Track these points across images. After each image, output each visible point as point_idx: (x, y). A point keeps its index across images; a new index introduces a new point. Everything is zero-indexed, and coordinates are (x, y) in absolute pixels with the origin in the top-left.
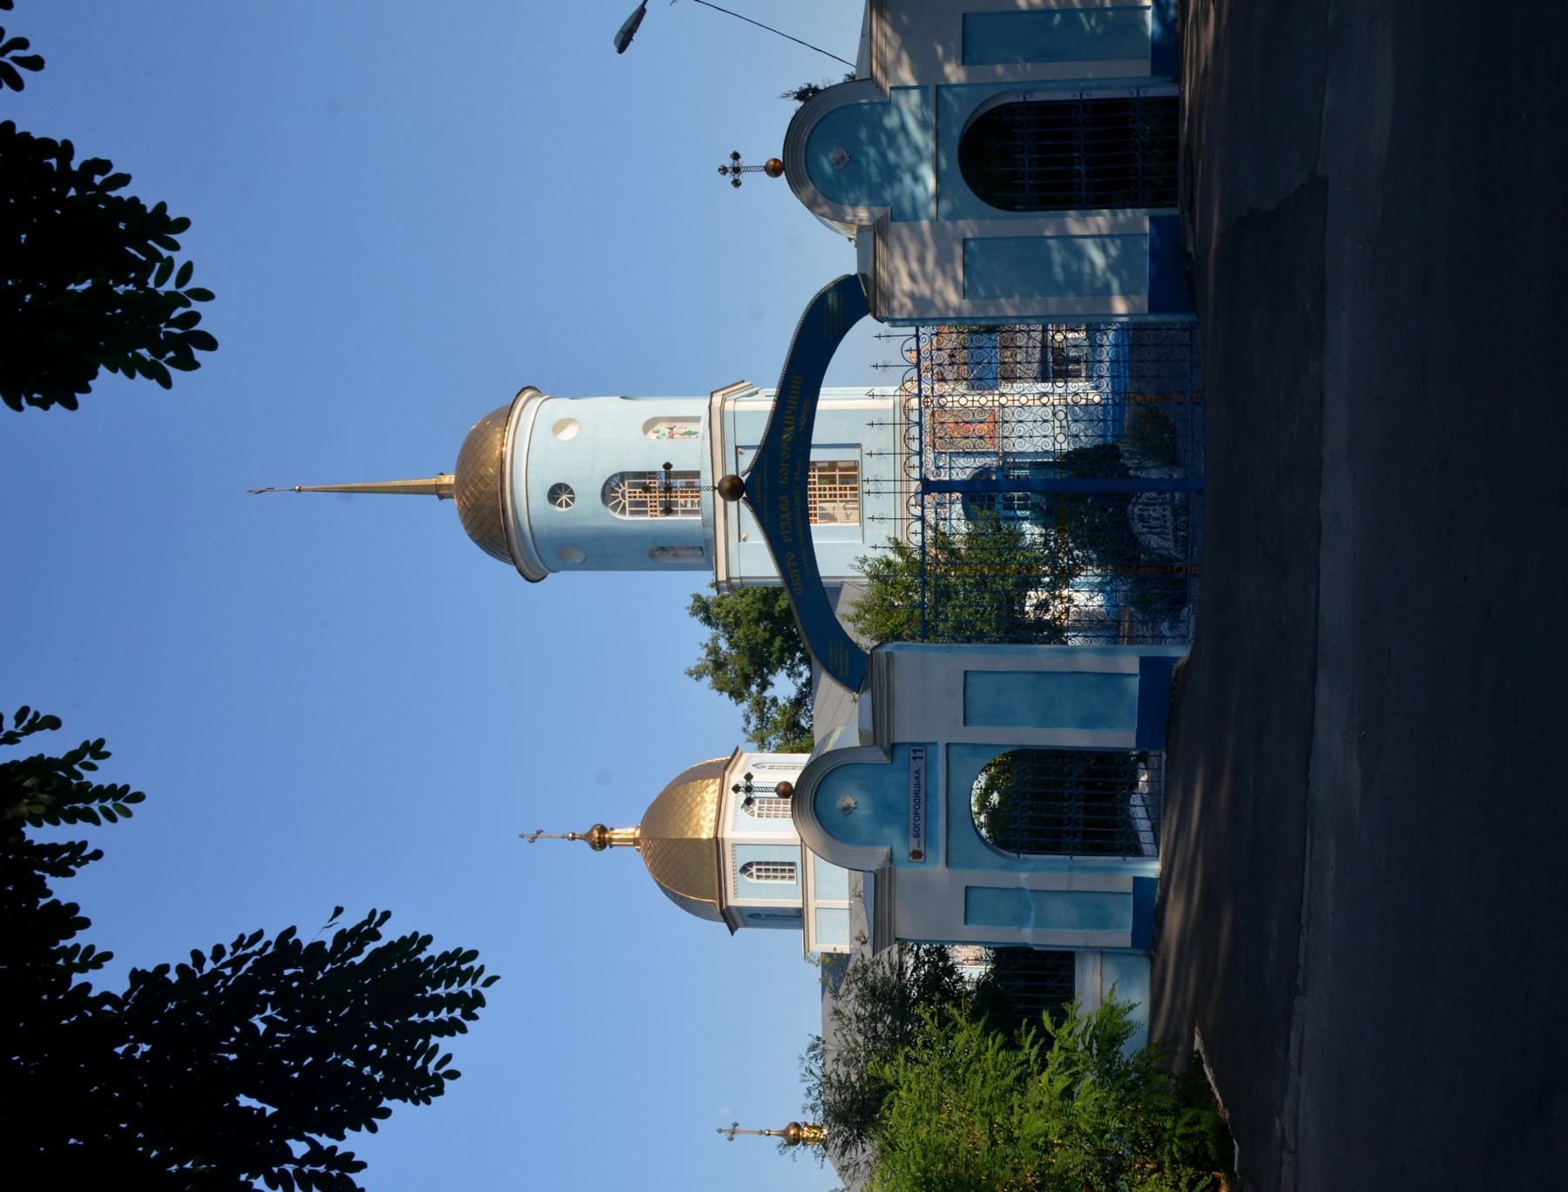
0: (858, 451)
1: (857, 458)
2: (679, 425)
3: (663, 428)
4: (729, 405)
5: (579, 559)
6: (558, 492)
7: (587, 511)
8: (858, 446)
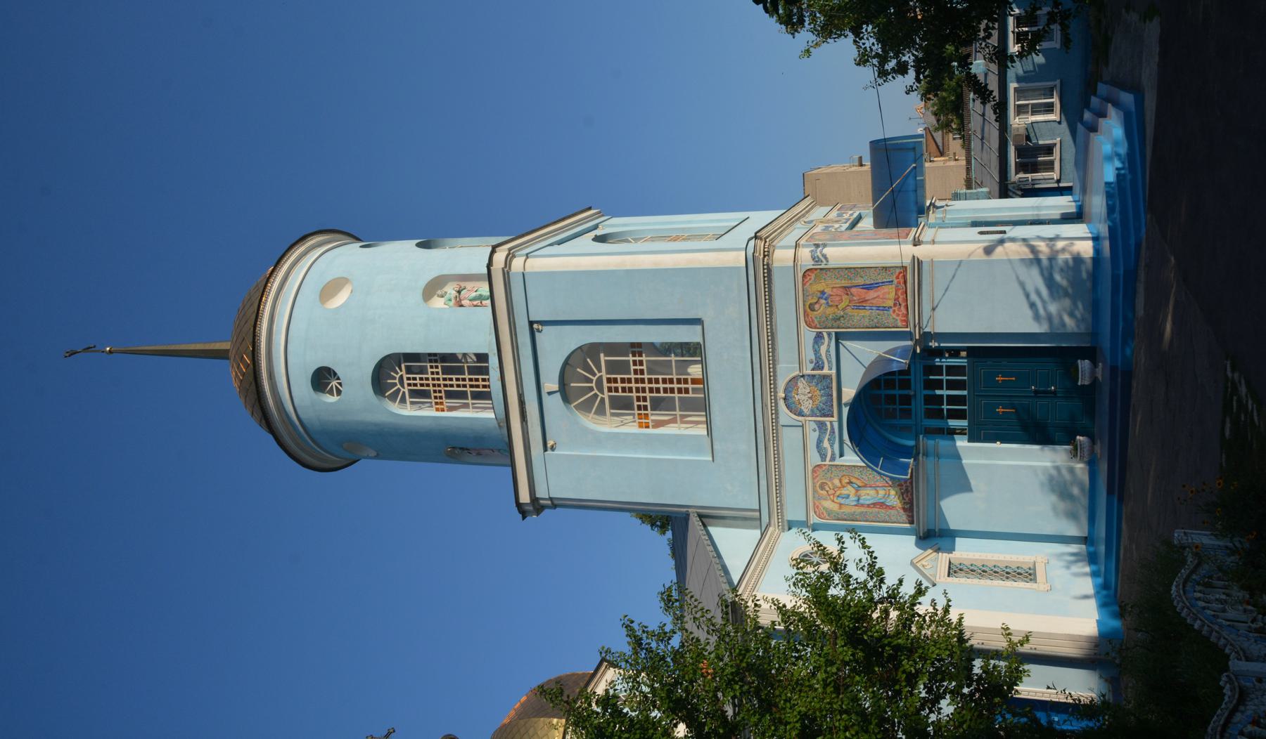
0: (699, 328)
1: (699, 339)
2: (469, 285)
3: (450, 290)
4: (517, 264)
5: (373, 454)
6: (322, 378)
7: (355, 401)
8: (698, 321)
